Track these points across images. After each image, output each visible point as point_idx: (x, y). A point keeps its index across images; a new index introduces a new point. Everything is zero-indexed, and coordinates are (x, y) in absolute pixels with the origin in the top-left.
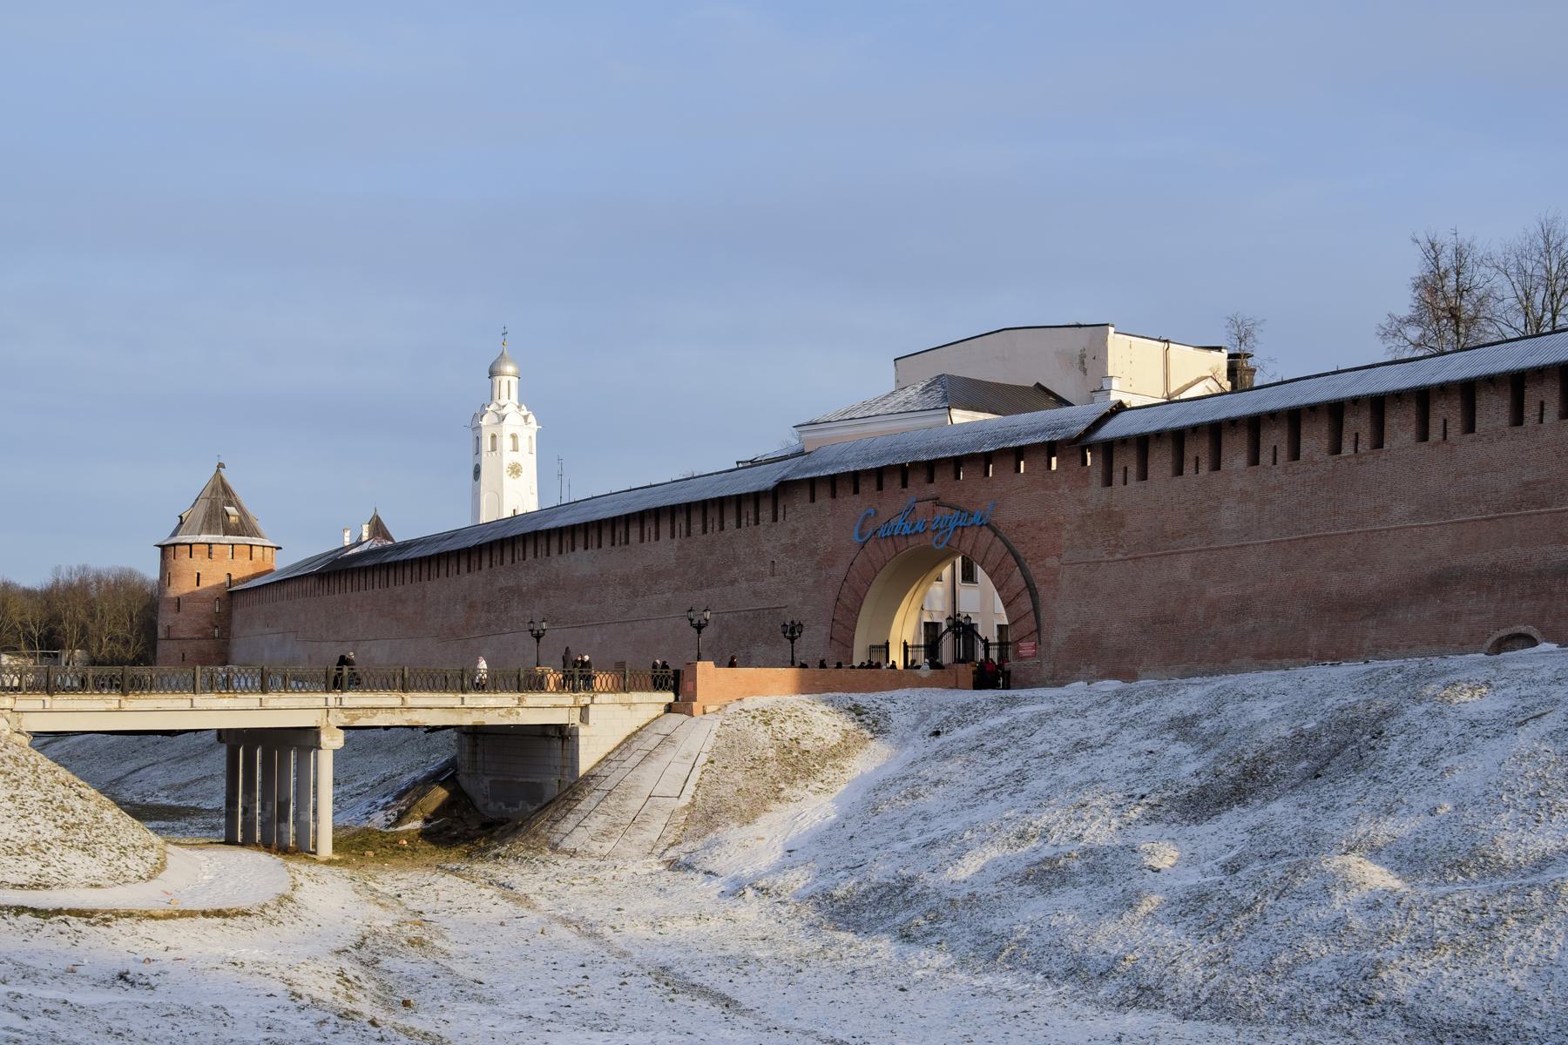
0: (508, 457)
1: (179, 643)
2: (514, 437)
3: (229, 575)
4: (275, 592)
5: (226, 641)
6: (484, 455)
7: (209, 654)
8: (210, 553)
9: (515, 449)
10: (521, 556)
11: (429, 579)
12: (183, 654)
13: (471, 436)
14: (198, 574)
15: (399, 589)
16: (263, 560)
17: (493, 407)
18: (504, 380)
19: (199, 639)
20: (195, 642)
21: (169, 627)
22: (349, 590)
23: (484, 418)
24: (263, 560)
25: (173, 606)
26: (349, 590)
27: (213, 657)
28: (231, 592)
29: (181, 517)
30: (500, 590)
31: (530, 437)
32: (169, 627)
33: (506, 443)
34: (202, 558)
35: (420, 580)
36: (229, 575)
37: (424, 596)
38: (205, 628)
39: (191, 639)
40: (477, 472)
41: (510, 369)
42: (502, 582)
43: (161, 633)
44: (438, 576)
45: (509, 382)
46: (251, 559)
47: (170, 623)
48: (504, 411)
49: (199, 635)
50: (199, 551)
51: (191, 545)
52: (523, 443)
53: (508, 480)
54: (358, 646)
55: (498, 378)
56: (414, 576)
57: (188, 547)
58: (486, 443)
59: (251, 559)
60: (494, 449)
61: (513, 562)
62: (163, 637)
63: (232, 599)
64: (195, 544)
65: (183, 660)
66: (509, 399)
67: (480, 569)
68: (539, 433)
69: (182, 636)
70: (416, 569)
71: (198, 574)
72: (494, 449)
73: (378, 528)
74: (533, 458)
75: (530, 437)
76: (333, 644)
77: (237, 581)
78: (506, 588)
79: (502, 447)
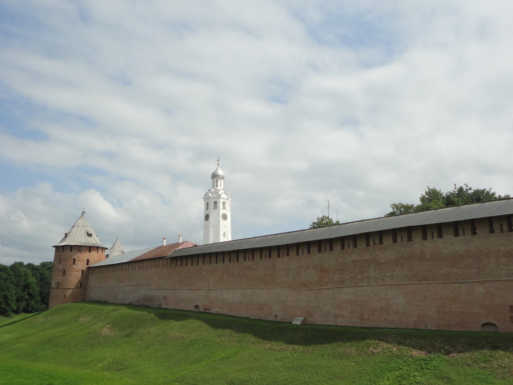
0: (222, 212)
2: (224, 203)
9: (224, 208)
11: (279, 257)
16: (102, 254)
21: (58, 283)
29: (66, 234)
30: (354, 262)
32: (58, 283)
43: (53, 285)
46: (98, 253)
47: (59, 281)
52: (227, 206)
53: (222, 221)
54: (210, 292)
57: (70, 247)
58: (212, 205)
59: (98, 253)
78: (360, 260)
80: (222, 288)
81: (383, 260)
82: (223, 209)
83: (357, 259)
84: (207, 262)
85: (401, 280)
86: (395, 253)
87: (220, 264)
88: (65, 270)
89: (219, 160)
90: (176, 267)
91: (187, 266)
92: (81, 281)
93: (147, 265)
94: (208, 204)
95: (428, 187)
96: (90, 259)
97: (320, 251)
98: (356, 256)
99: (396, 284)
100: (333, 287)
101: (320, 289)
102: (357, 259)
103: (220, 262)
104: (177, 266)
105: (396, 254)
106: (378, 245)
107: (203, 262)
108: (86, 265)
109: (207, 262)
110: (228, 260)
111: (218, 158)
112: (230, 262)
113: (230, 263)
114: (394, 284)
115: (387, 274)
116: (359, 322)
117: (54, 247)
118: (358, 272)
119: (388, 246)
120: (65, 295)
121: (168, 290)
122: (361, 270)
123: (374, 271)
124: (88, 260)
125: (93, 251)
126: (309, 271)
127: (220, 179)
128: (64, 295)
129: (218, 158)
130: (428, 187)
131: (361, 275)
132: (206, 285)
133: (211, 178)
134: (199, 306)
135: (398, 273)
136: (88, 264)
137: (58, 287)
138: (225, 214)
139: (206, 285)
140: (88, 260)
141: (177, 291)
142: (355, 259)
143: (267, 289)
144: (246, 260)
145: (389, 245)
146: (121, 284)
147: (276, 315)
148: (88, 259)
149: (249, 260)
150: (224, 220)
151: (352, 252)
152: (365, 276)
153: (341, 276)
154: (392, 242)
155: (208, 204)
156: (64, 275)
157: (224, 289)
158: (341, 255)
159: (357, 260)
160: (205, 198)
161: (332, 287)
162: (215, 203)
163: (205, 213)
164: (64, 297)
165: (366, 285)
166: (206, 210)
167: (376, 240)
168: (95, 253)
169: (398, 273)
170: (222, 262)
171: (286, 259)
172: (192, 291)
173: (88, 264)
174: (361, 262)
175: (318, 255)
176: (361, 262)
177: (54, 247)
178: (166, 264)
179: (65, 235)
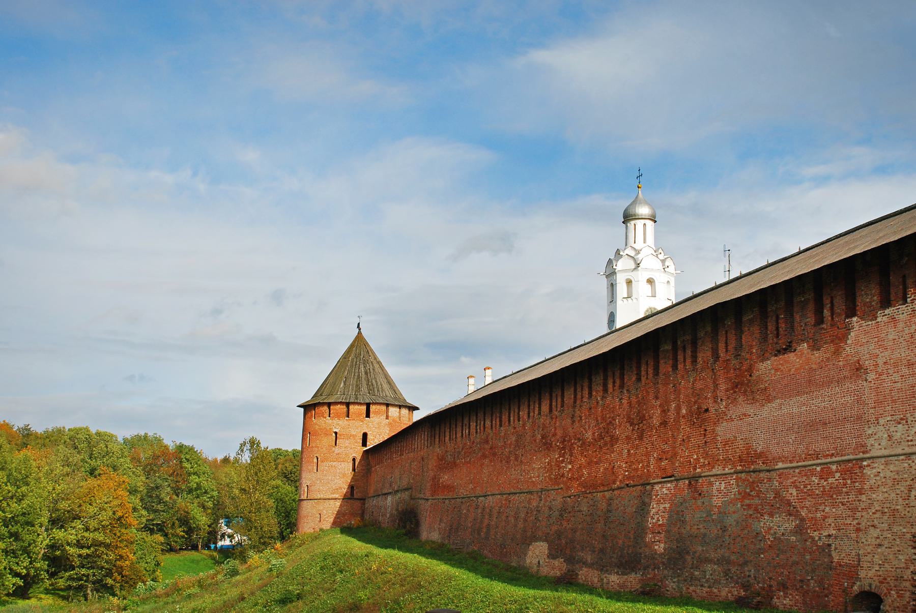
6: (619, 302)
45: (645, 224)
46: (387, 417)
58: (621, 290)
59: (387, 417)
71: (336, 433)
84: (439, 436)
88: (319, 460)
89: (642, 175)
94: (612, 285)
95: (359, 324)
96: (368, 433)
108: (361, 445)
109: (439, 436)
117: (297, 406)
124: (365, 436)
125: (376, 413)
127: (643, 221)
130: (359, 324)
133: (623, 222)
136: (364, 444)
140: (365, 436)
148: (364, 431)
155: (612, 285)
163: (608, 309)
168: (382, 417)
173: (364, 444)
177: (297, 406)
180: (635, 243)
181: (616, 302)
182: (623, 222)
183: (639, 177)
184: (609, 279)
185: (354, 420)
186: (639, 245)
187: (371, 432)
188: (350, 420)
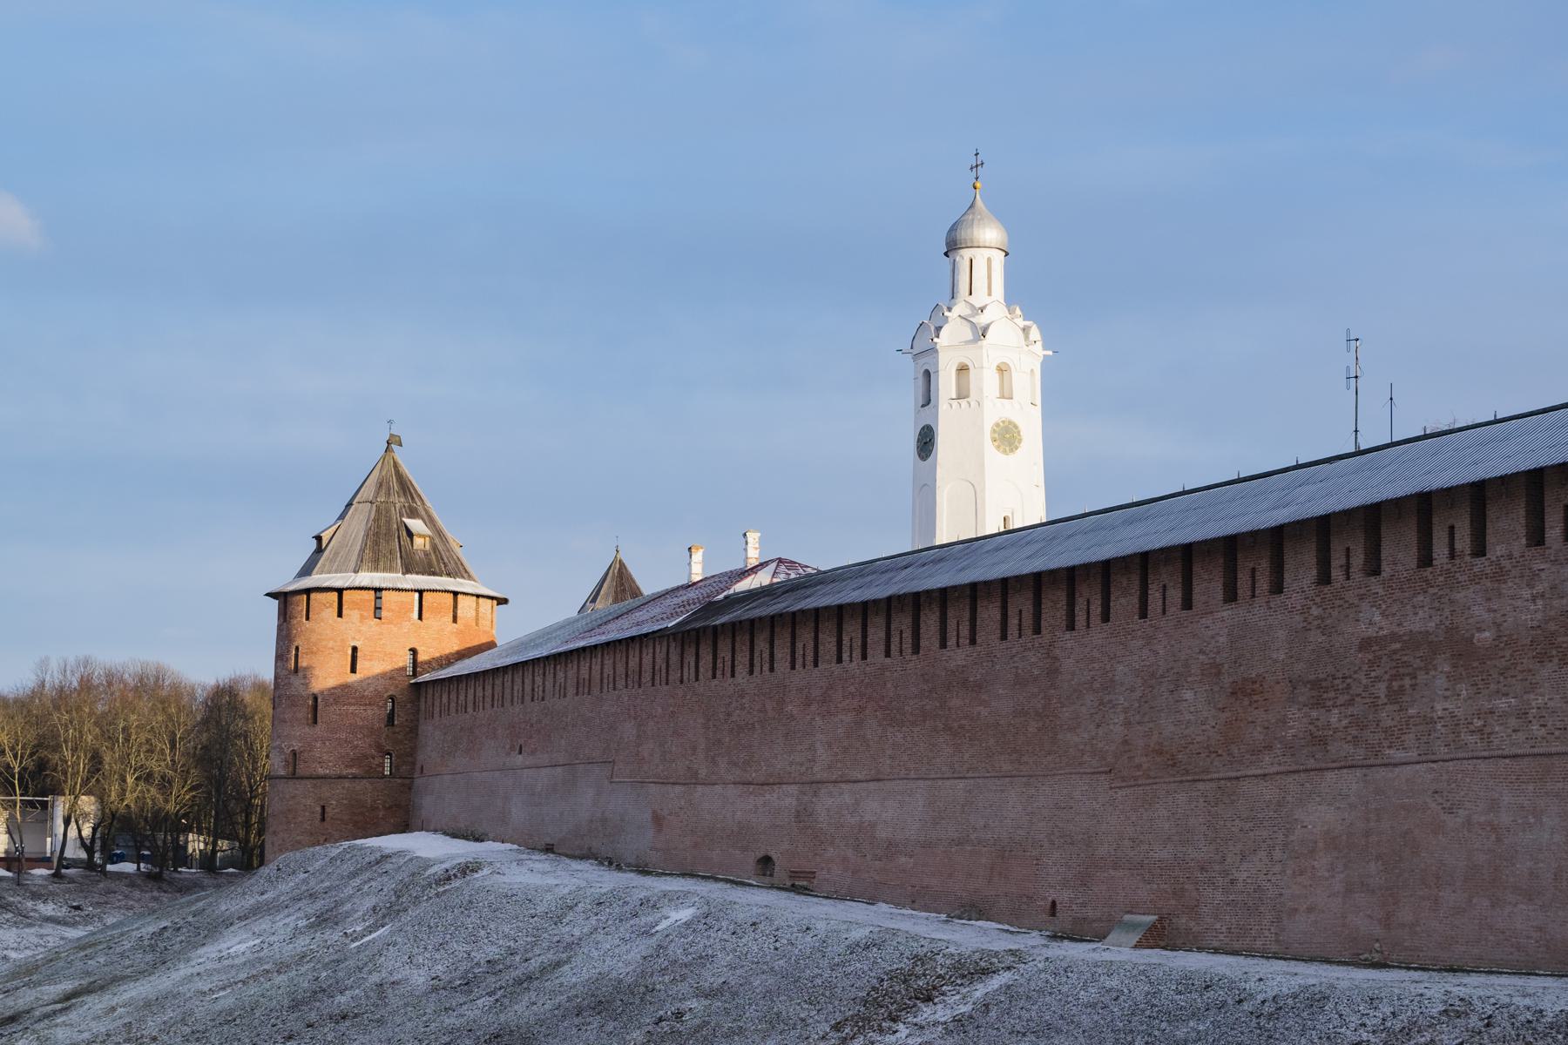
1: (315, 786)
2: (1002, 370)
3: (414, 651)
4: (539, 680)
5: (407, 781)
6: (943, 406)
7: (374, 809)
8: (378, 608)
9: (1006, 394)
10: (1464, 542)
11: (1071, 627)
12: (323, 808)
13: (909, 370)
14: (355, 649)
15: (959, 656)
16: (477, 625)
17: (960, 309)
18: (980, 257)
19: (355, 777)
20: (347, 784)
21: (294, 753)
22: (782, 665)
23: (942, 333)
24: (477, 625)
25: (303, 713)
26: (782, 665)
27: (381, 814)
28: (416, 684)
29: (319, 538)
30: (1365, 644)
31: (1032, 370)
32: (294, 753)
33: (986, 382)
34: (362, 618)
35: (1037, 630)
36: (414, 651)
37: (1053, 672)
38: (365, 757)
39: (340, 777)
40: (926, 442)
41: (989, 234)
42: (1372, 621)
44: (1106, 618)
45: (989, 260)
46: (455, 620)
47: (296, 746)
48: (982, 320)
49: (354, 771)
50: (356, 605)
51: (340, 591)
53: (993, 456)
54: (815, 794)
55: (966, 254)
56: (895, 640)
57: (335, 595)
58: (946, 384)
59: (455, 620)
60: (962, 394)
61: (1426, 560)
62: (282, 773)
63: (418, 699)
64: (347, 589)
65: (323, 819)
66: (990, 294)
67: (1277, 588)
68: (1046, 364)
69: (321, 771)
70: (902, 622)
71: (355, 649)
72: (962, 394)
73: (620, 582)
74: (1037, 413)
75: (1032, 370)
76: (732, 791)
77: (429, 663)
78: (1394, 637)
79: (981, 390)
80: (860, 777)
81: (1487, 634)
82: (1003, 397)
83: (1381, 628)
85: (1557, 733)
86: (1534, 599)
87: (854, 664)
88: (319, 700)
90: (697, 679)
91: (733, 675)
92: (388, 748)
93: (602, 673)
94: (927, 374)
97: (1231, 596)
98: (1377, 618)
99: (1536, 750)
100: (1282, 769)
101: (1230, 779)
102: (1381, 628)
103: (851, 656)
104: (701, 677)
105: (1540, 602)
106: (1468, 558)
107: (789, 658)
110: (883, 647)
111: (977, 154)
112: (888, 654)
113: (888, 660)
114: (1529, 751)
115: (1502, 704)
116: (1377, 940)
117: (267, 595)
118: (1383, 696)
119: (1506, 563)
120: (323, 807)
121: (669, 787)
122: (1395, 684)
123: (1446, 690)
126: (1189, 695)
128: (319, 809)
129: (977, 154)
131: (1396, 707)
132: (802, 765)
133: (946, 254)
134: (774, 857)
135: (1547, 697)
137: (294, 774)
138: (1010, 422)
139: (802, 765)
141: (699, 788)
142: (1371, 632)
143: (1024, 779)
144: (949, 644)
145: (1510, 557)
146: (519, 760)
147: (1054, 904)
149: (958, 646)
150: (1005, 452)
151: (1362, 597)
152: (1411, 711)
153: (1314, 714)
154: (1524, 541)
155: (927, 374)
156: (315, 722)
157: (867, 781)
158: (1315, 611)
159: (1381, 633)
160: (915, 351)
161: (1275, 769)
162: (963, 369)
164: (319, 816)
165: (1413, 755)
166: (923, 406)
167: (1457, 536)
169: (1547, 697)
170: (857, 653)
171: (1099, 635)
172: (751, 788)
174: (1398, 646)
175: (1225, 614)
176: (1398, 646)
177: (267, 595)
178: (664, 666)
179: (315, 541)
180: (971, 294)
181: (936, 407)
182: (946, 254)
183: (977, 166)
184: (922, 361)
185: (392, 623)
186: (979, 298)
187: (423, 648)
188: (383, 624)
